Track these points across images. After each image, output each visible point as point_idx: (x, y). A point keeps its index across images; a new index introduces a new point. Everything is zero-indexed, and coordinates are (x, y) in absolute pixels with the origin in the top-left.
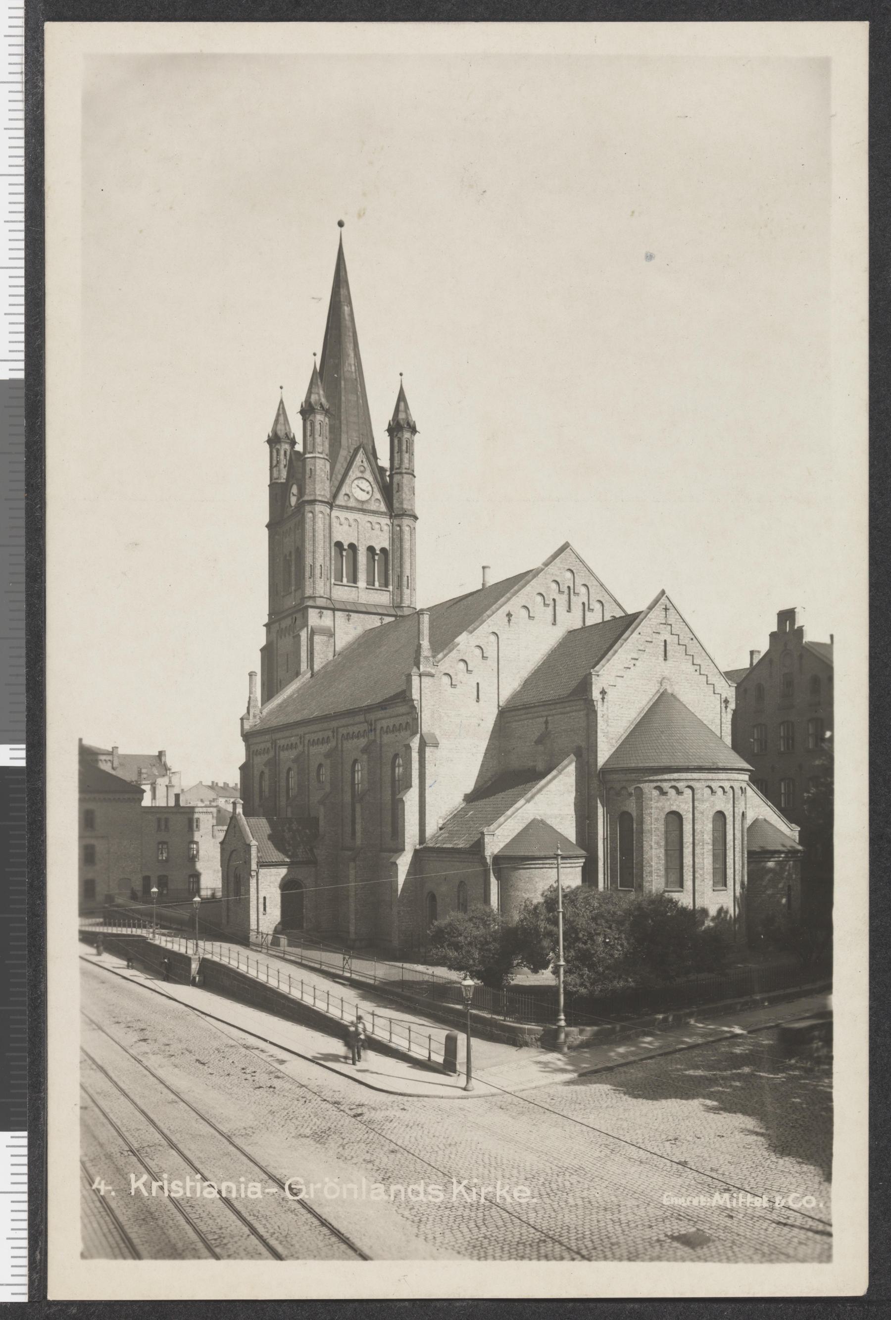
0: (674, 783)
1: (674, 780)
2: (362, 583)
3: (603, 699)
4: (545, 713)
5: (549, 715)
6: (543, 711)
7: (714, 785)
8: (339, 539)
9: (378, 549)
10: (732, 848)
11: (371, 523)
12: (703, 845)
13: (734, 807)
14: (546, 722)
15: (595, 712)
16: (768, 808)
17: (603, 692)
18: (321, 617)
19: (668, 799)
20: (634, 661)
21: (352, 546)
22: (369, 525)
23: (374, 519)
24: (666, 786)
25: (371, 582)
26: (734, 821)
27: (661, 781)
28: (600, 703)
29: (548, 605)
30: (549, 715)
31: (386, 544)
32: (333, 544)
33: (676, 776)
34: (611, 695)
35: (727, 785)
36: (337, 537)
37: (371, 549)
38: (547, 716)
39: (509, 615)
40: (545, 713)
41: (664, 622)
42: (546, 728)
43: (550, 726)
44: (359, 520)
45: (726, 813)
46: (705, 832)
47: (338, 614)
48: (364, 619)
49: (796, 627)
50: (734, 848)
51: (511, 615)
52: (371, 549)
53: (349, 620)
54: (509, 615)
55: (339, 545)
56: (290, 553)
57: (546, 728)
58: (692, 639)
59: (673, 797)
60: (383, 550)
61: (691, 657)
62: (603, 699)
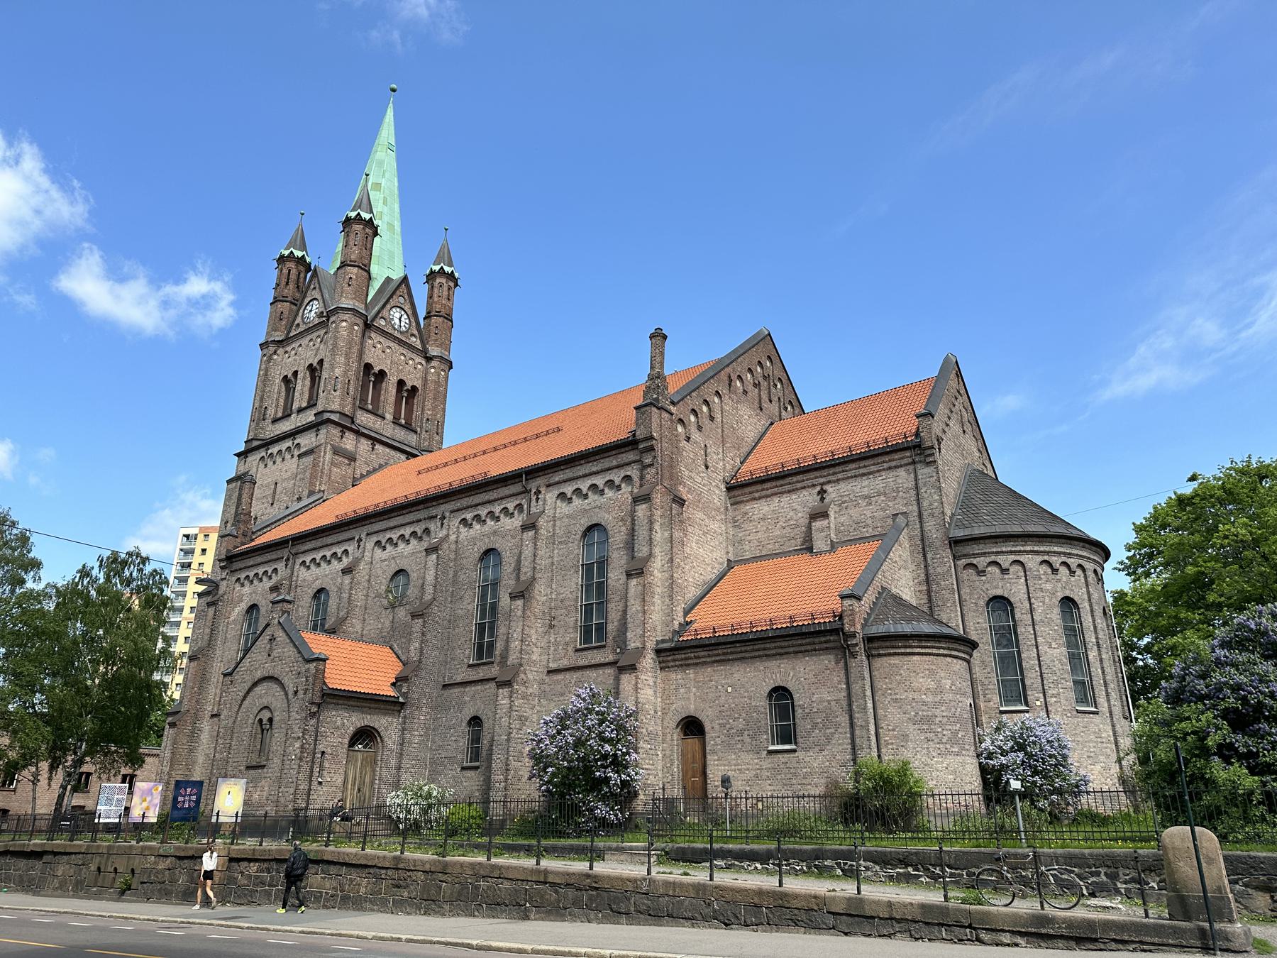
2: (389, 417)
4: (822, 480)
5: (829, 482)
6: (816, 478)
8: (370, 361)
9: (409, 384)
11: (405, 356)
18: (342, 437)
21: (382, 374)
22: (402, 357)
23: (410, 354)
25: (396, 421)
27: (1048, 553)
31: (418, 384)
32: (363, 364)
36: (368, 359)
37: (401, 383)
38: (822, 484)
40: (822, 480)
43: (828, 499)
47: (363, 440)
48: (389, 453)
52: (401, 383)
53: (373, 449)
55: (368, 367)
56: (295, 373)
57: (822, 499)
59: (1064, 579)
60: (414, 389)
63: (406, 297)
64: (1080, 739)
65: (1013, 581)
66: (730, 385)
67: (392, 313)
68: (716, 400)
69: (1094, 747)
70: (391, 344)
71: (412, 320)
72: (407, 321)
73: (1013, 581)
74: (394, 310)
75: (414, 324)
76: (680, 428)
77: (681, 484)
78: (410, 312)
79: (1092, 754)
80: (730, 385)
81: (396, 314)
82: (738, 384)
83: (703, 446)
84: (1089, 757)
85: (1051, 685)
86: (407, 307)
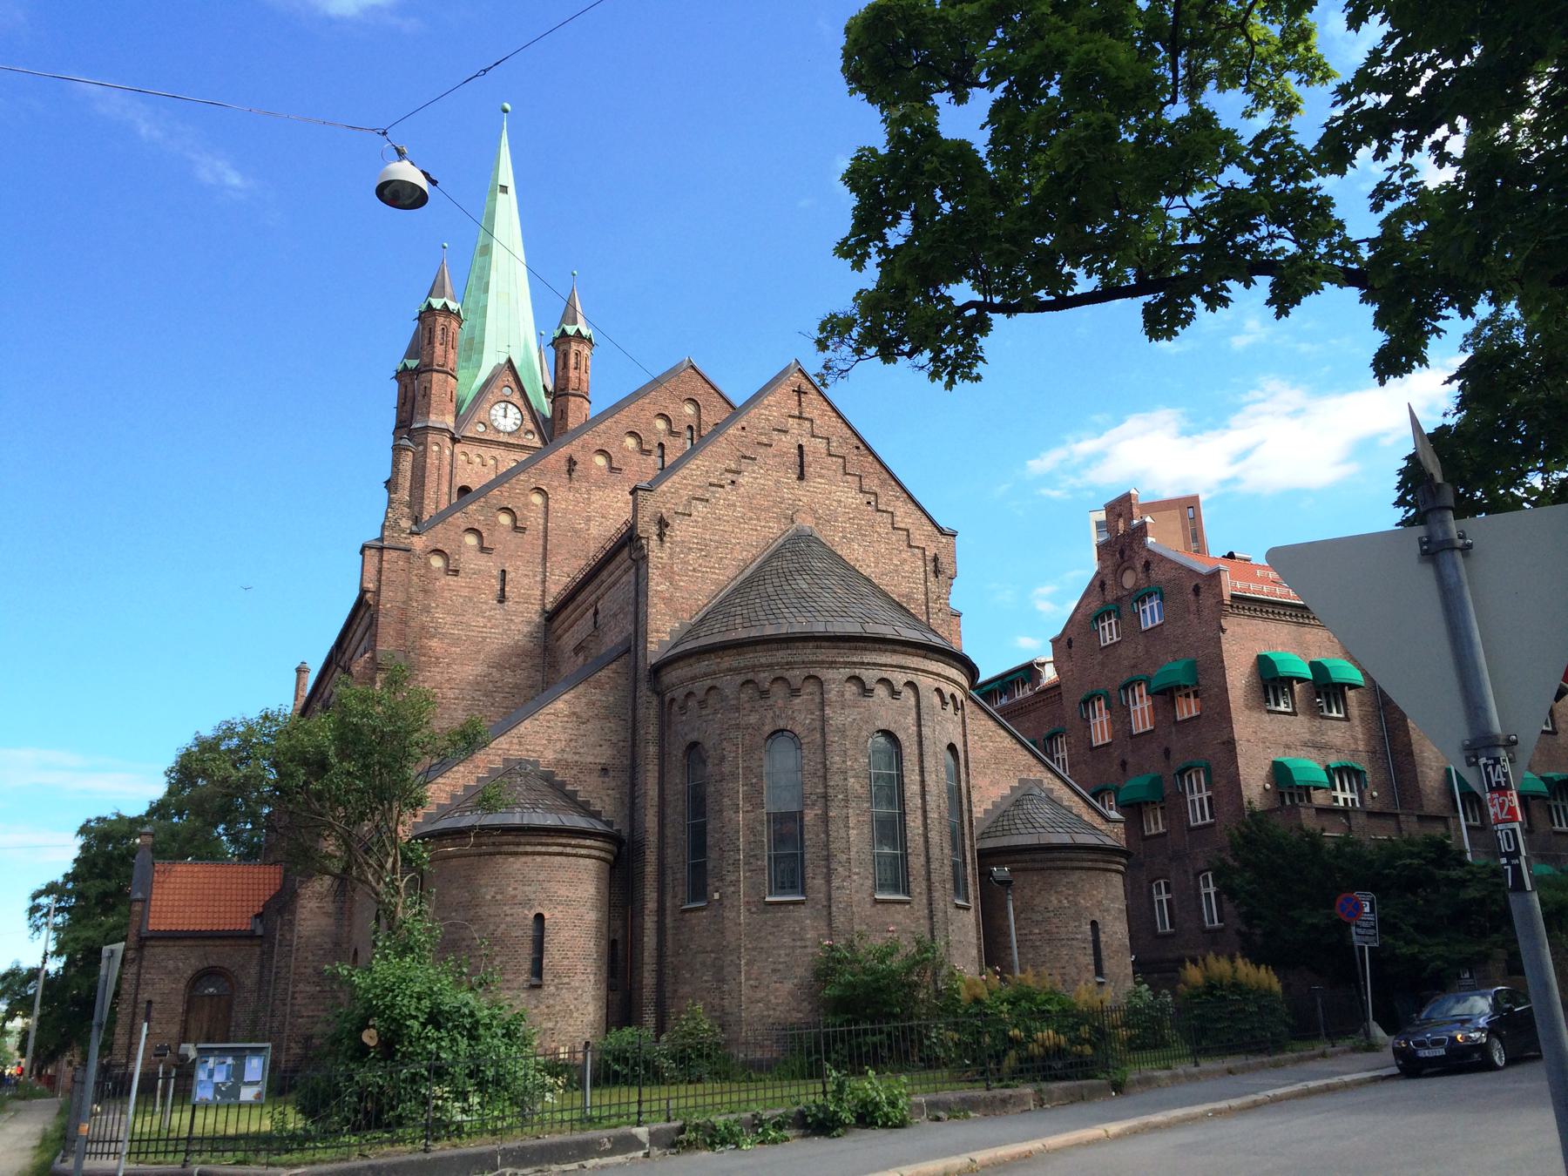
0: (779, 673)
1: (781, 665)
3: (661, 536)
5: (599, 598)
7: (869, 675)
8: (467, 482)
10: (919, 812)
12: (846, 800)
13: (919, 726)
14: (596, 613)
15: (645, 558)
16: (991, 723)
17: (663, 524)
19: (771, 707)
20: (730, 476)
24: (764, 677)
26: (921, 755)
28: (654, 542)
29: (649, 452)
30: (599, 598)
32: (455, 490)
33: (781, 655)
34: (680, 530)
35: (899, 678)
36: (460, 481)
39: (572, 462)
41: (797, 413)
42: (595, 623)
44: (498, 457)
45: (901, 736)
46: (851, 773)
49: (990, 315)
50: (925, 812)
51: (575, 463)
54: (572, 462)
58: (858, 448)
61: (858, 478)
62: (661, 536)
63: (513, 385)
64: (765, 945)
65: (710, 717)
66: (570, 471)
67: (493, 412)
68: (537, 499)
69: (787, 955)
70: (496, 452)
71: (525, 412)
72: (519, 416)
73: (710, 717)
74: (496, 407)
75: (527, 417)
76: (437, 562)
77: (433, 636)
78: (520, 403)
79: (781, 967)
80: (570, 471)
81: (498, 411)
82: (600, 461)
83: (496, 572)
84: (774, 971)
85: (731, 868)
86: (516, 398)
